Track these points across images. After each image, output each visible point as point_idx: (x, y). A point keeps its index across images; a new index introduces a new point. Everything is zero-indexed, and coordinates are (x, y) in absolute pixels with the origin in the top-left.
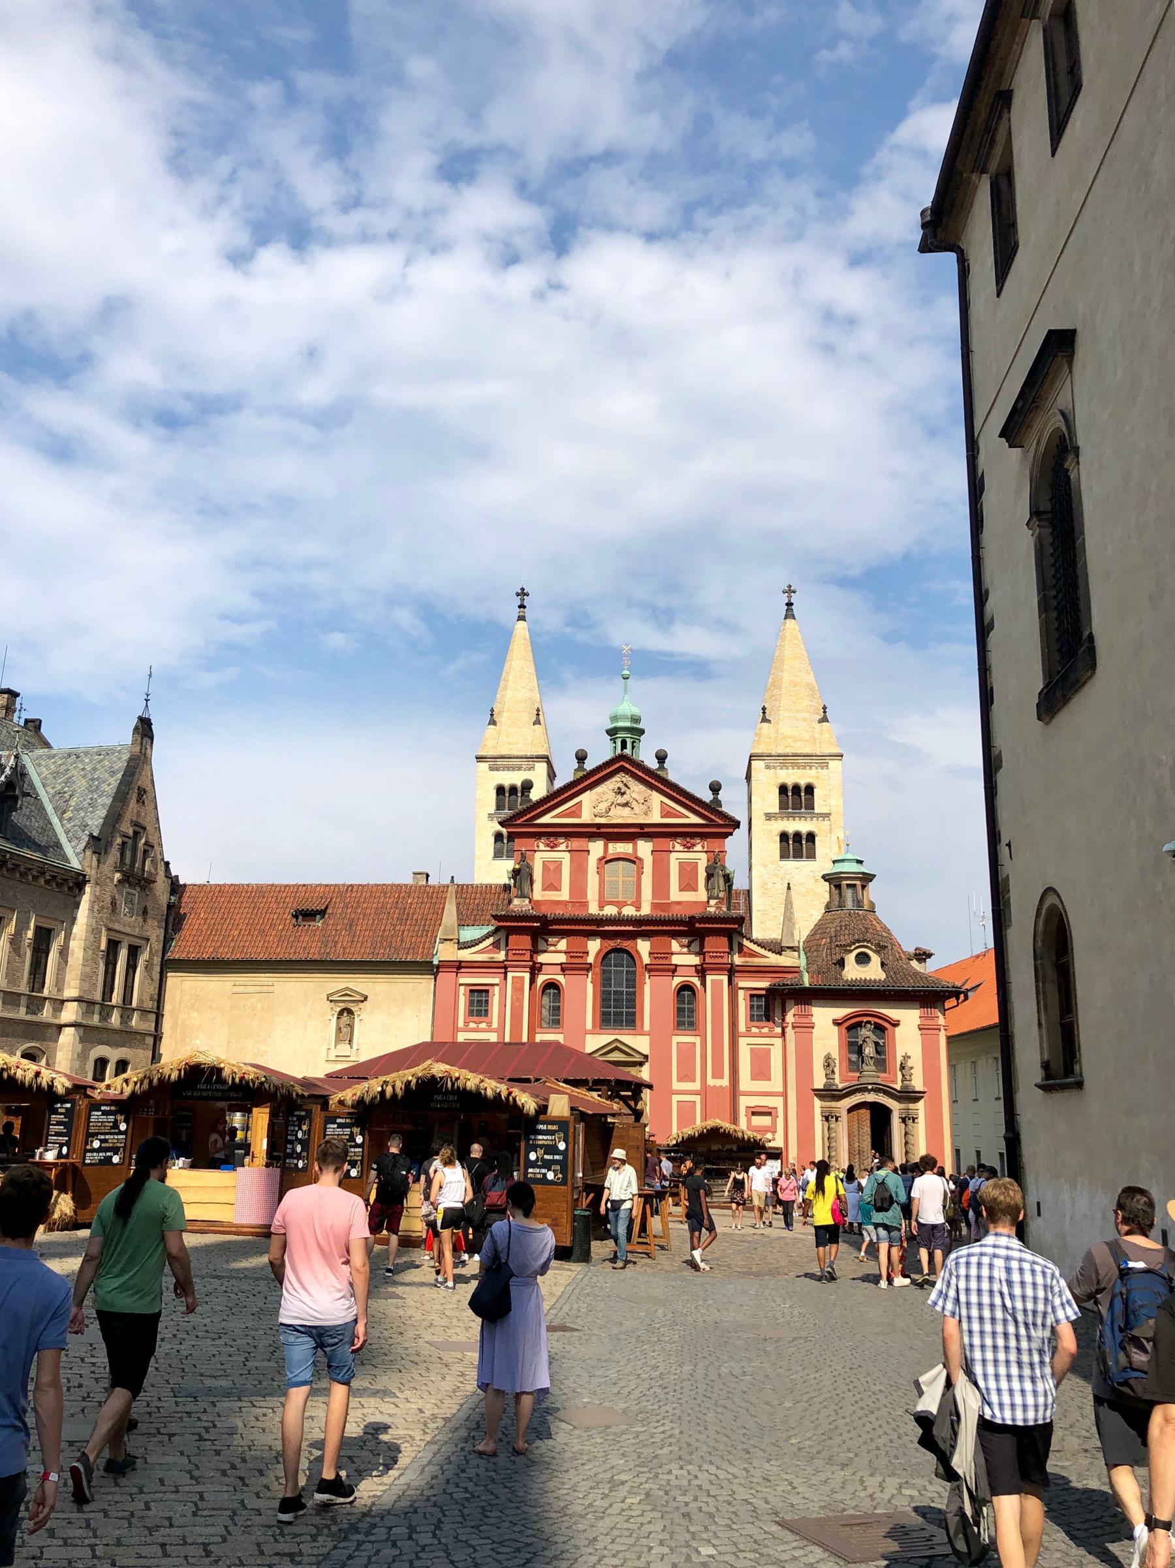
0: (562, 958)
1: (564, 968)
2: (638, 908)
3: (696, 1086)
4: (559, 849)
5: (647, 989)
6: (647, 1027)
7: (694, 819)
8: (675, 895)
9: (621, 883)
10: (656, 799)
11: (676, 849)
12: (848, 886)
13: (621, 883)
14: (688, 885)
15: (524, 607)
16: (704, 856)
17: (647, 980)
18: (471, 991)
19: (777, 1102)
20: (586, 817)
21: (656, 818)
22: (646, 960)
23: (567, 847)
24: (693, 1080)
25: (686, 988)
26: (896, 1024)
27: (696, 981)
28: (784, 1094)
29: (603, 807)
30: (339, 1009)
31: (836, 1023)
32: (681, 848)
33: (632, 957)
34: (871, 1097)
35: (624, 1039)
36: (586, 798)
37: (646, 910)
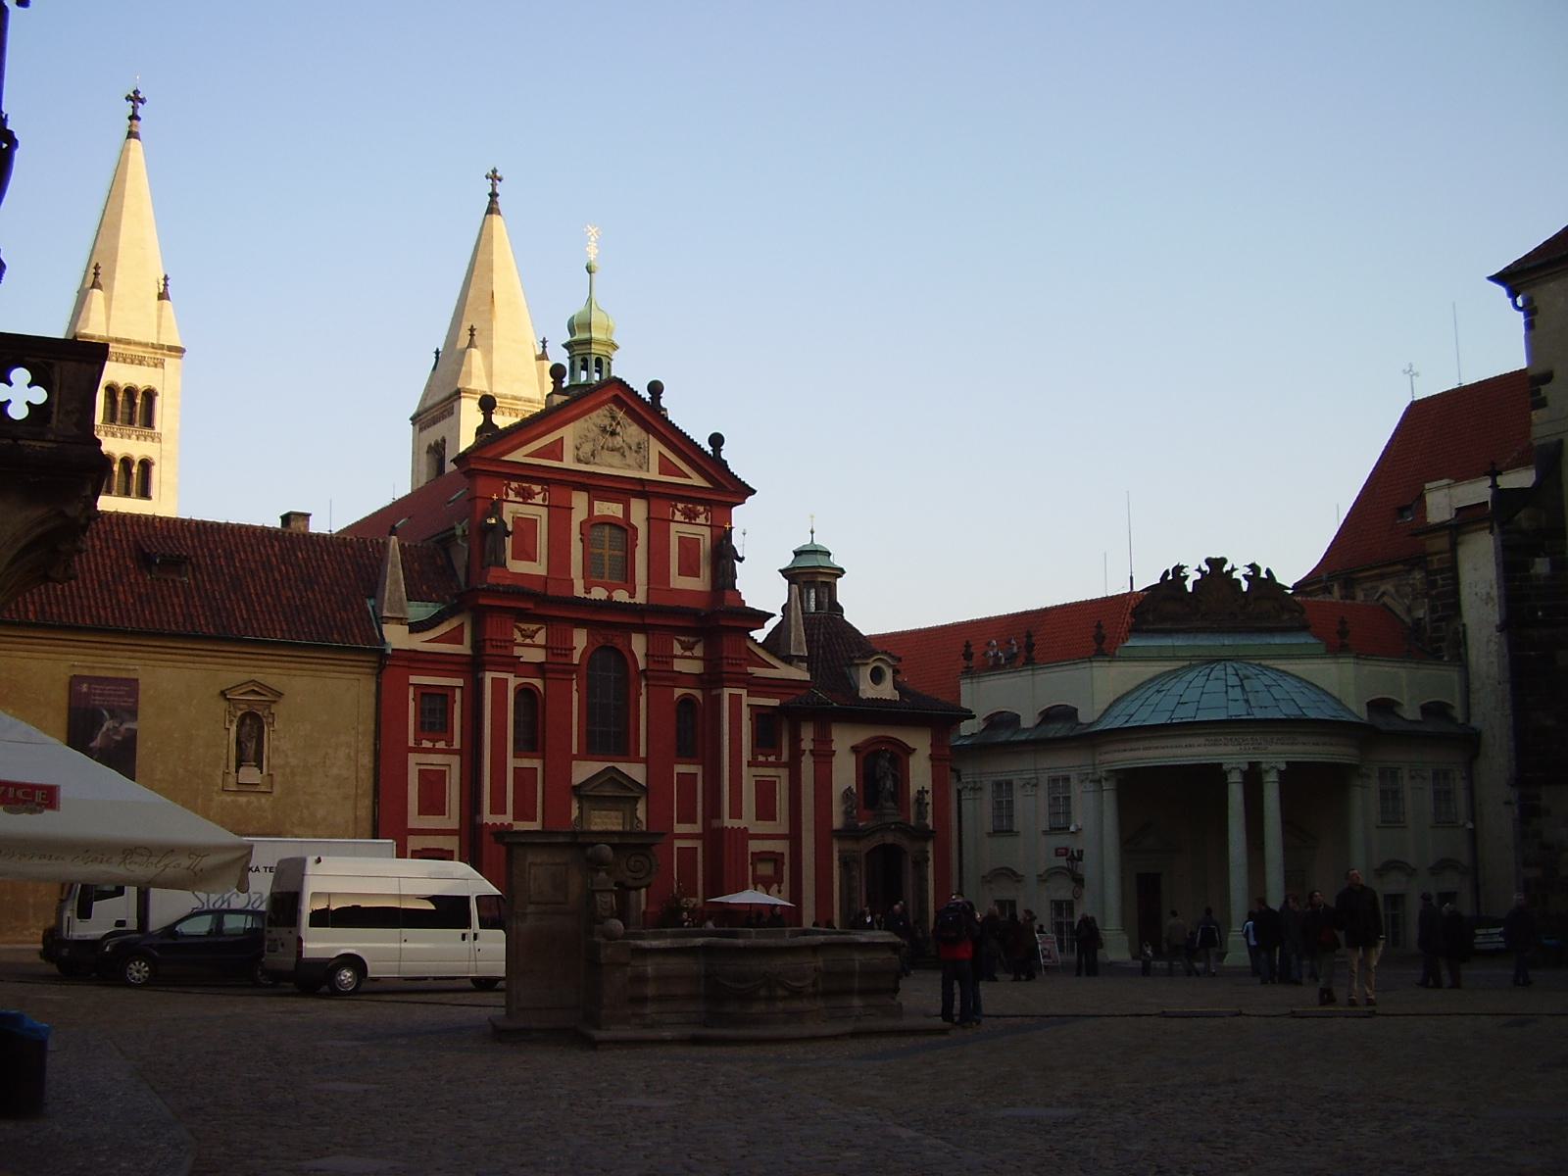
0: (537, 656)
1: (539, 669)
2: (632, 596)
3: (697, 828)
4: (534, 501)
5: (643, 700)
6: (643, 753)
7: (697, 480)
8: (679, 582)
9: (606, 558)
10: (656, 447)
11: (676, 519)
12: (822, 582)
13: (606, 558)
14: (689, 568)
15: (138, 119)
16: (707, 531)
17: (644, 691)
18: (423, 694)
19: (781, 847)
20: (568, 462)
21: (653, 474)
22: (642, 665)
23: (544, 500)
24: (694, 822)
25: (686, 700)
26: (910, 751)
27: (698, 694)
28: (794, 837)
29: (587, 448)
30: (239, 713)
31: (855, 749)
32: (682, 519)
33: (624, 657)
34: (890, 839)
35: (622, 767)
36: (569, 434)
37: (640, 598)
